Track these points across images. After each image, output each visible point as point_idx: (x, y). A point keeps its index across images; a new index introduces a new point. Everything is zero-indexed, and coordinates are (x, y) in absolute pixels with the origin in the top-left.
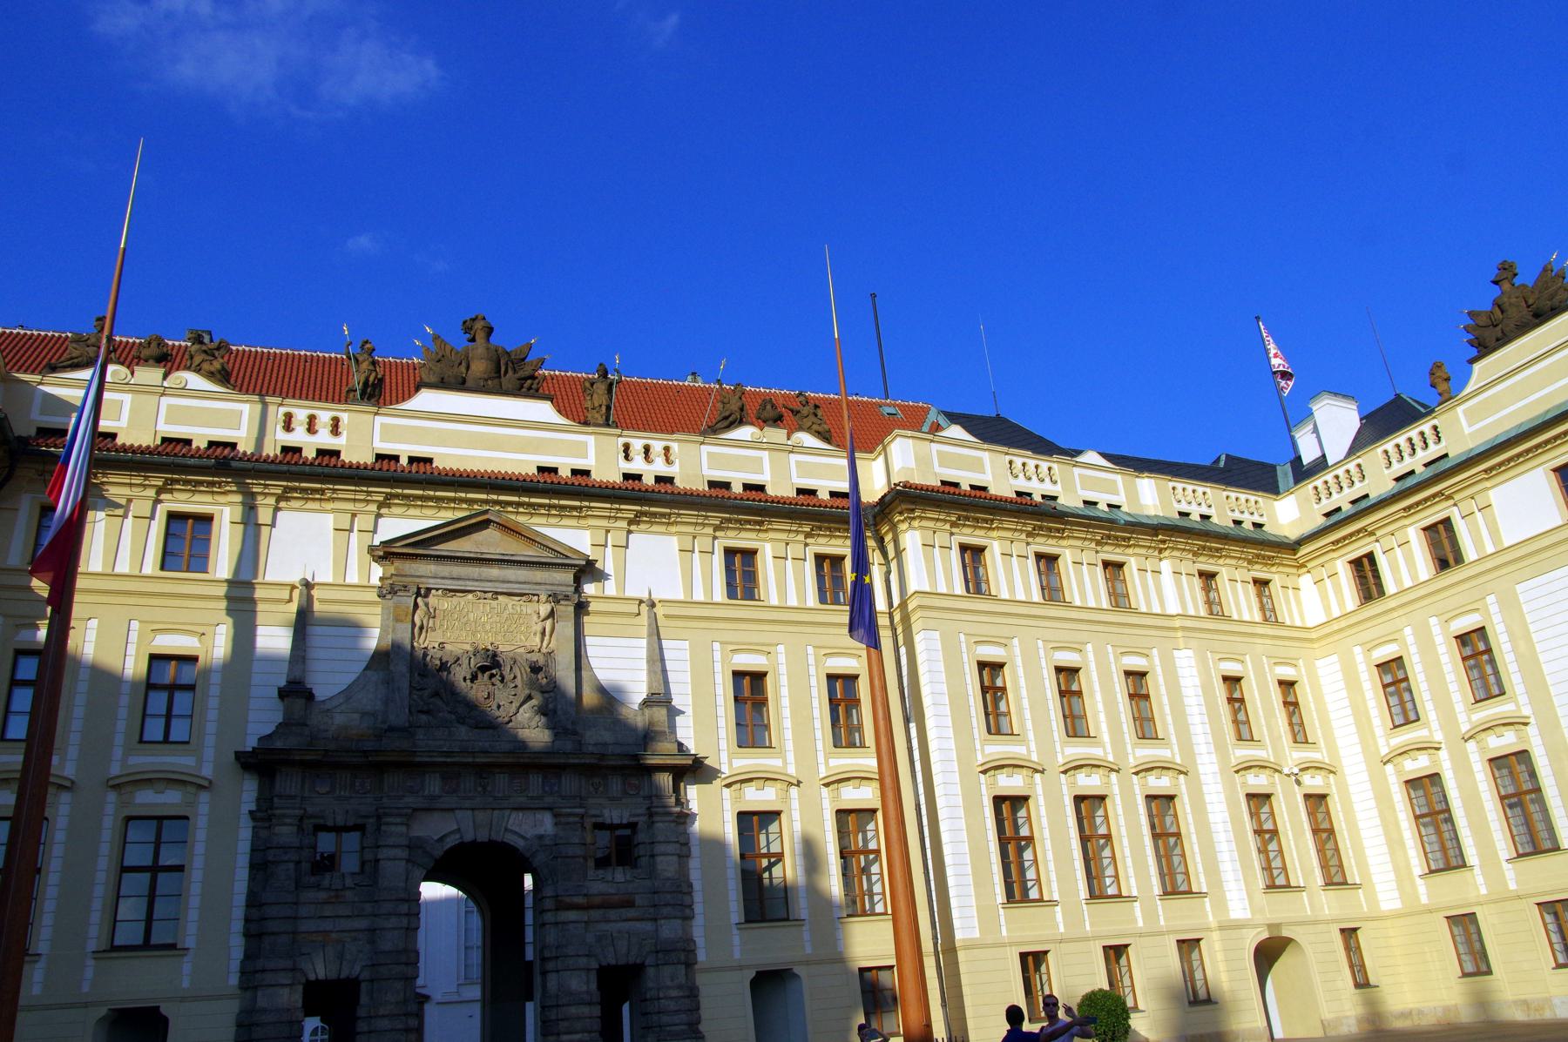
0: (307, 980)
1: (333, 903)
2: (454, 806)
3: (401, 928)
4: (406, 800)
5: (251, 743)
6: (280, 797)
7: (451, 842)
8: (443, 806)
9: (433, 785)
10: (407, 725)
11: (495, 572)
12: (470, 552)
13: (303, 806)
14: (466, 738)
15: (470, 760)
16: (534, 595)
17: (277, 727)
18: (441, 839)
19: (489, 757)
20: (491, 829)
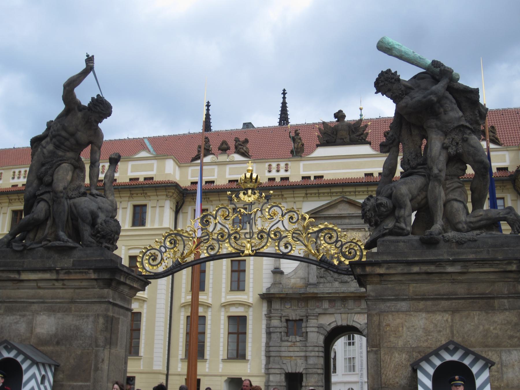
0: (286, 372)
1: (293, 346)
2: (333, 312)
3: (316, 356)
4: (317, 310)
5: (264, 291)
6: (273, 310)
7: (333, 325)
8: (330, 312)
9: (326, 305)
10: (316, 282)
11: (347, 221)
12: (336, 214)
13: (282, 313)
14: (338, 287)
15: (338, 295)
16: (363, 228)
17: (271, 285)
18: (329, 324)
19: (344, 294)
20: (347, 321)
